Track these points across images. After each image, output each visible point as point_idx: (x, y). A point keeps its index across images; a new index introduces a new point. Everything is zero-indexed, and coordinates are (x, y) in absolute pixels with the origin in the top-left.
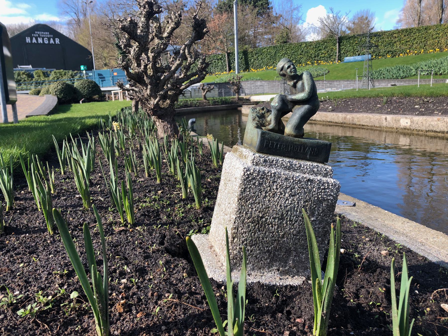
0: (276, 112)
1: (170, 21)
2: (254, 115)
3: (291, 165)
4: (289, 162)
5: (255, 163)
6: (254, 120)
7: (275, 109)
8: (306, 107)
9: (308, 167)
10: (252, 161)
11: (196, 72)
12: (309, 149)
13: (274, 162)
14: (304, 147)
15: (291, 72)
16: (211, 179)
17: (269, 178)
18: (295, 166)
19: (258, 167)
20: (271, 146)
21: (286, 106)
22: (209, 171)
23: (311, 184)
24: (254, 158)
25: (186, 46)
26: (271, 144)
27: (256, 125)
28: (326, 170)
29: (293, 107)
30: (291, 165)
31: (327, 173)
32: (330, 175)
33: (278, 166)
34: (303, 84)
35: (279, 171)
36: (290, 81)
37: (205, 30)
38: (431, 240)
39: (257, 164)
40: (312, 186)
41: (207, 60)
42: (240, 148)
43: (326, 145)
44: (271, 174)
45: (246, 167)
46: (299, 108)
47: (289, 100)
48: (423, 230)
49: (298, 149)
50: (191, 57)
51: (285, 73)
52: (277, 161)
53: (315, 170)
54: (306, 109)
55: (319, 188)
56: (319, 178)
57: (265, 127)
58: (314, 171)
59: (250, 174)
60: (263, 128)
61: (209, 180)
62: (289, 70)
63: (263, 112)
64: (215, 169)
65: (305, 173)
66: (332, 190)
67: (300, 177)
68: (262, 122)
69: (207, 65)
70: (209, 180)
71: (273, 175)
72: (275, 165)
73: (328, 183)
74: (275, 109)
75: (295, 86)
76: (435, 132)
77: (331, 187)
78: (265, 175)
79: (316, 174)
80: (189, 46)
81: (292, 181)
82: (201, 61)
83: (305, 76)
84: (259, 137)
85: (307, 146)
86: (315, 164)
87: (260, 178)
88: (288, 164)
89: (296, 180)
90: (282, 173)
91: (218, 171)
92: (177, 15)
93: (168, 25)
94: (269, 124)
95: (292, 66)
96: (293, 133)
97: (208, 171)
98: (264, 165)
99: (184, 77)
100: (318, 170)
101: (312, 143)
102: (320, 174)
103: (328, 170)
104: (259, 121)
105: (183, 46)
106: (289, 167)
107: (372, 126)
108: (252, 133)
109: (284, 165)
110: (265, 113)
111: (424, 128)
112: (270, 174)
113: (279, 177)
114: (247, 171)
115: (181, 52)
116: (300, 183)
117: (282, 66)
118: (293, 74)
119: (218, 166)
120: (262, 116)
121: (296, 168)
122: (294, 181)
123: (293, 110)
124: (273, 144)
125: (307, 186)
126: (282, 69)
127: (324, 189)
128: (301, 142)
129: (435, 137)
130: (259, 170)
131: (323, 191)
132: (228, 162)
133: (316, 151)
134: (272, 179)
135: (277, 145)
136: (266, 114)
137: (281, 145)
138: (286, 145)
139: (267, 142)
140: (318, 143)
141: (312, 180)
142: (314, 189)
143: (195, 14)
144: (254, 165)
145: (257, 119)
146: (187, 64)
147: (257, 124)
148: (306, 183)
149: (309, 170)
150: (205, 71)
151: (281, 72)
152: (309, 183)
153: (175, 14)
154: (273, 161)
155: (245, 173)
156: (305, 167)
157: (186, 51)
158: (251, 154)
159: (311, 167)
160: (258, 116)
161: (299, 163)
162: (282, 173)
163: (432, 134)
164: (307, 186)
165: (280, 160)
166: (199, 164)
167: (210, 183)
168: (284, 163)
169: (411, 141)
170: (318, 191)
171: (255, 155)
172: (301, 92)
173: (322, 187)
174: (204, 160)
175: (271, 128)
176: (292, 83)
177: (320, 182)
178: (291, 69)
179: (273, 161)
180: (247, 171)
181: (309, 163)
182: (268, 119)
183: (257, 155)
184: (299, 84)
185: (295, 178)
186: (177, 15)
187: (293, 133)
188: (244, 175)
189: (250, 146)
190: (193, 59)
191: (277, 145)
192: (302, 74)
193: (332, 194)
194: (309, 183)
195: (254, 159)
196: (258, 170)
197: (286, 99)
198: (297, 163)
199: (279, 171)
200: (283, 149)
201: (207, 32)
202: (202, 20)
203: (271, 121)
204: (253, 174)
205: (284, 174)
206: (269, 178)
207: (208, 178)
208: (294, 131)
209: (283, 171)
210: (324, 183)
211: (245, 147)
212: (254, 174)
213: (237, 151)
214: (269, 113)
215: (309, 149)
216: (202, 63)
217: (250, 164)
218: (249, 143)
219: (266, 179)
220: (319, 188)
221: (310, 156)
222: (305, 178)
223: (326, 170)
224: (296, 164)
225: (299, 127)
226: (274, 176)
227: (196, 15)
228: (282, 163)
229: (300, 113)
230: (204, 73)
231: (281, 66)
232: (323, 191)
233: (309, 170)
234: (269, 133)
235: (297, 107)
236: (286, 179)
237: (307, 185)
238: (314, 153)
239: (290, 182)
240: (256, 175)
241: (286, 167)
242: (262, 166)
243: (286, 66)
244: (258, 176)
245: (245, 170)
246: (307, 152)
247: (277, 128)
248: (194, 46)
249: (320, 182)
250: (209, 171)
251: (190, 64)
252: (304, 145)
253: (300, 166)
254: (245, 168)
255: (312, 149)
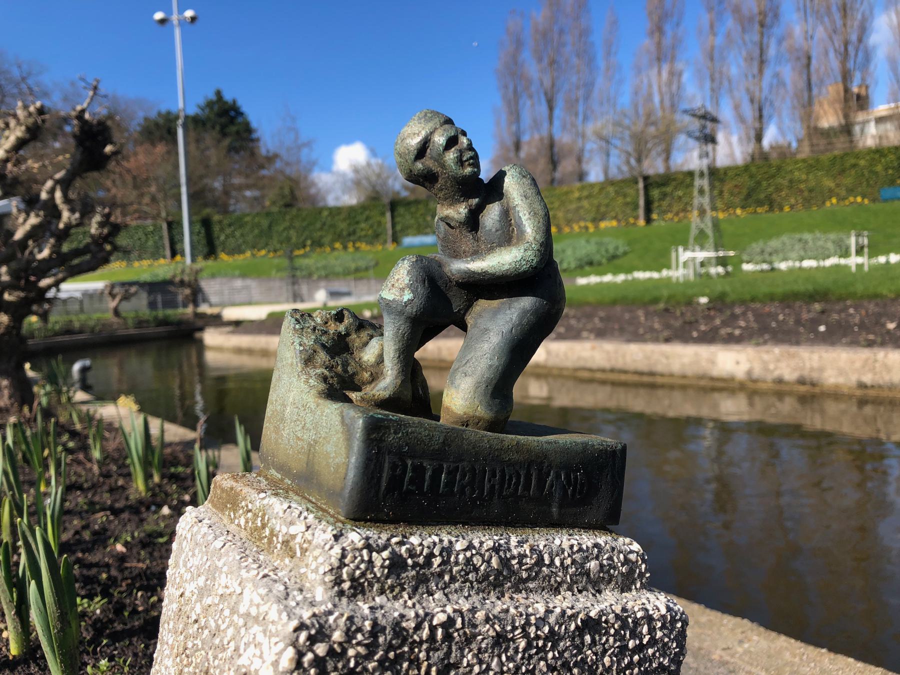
0: (404, 327)
1: (12, 122)
2: (309, 341)
3: (505, 562)
4: (496, 549)
5: (346, 586)
6: (308, 361)
7: (401, 313)
8: (526, 303)
9: (568, 561)
10: (329, 578)
11: (87, 246)
12: (558, 476)
13: (437, 561)
14: (540, 470)
15: (460, 162)
16: (126, 544)
17: (422, 655)
18: (520, 563)
19: (365, 608)
20: (412, 481)
21: (441, 306)
22: (122, 511)
23: (593, 640)
24: (343, 556)
25: (57, 182)
26: (409, 477)
27: (322, 386)
28: (627, 561)
29: (469, 306)
30: (505, 562)
31: (631, 571)
32: (641, 575)
33: (453, 579)
34: (507, 214)
35: (465, 606)
36: (453, 201)
37: (108, 149)
38: (740, 650)
39: (358, 589)
40: (599, 648)
41: (117, 218)
42: (253, 495)
43: (614, 452)
44: (433, 629)
45: (306, 614)
46: (496, 312)
47: (456, 277)
48: (703, 619)
49: (517, 484)
50: (72, 211)
51: (436, 168)
52: (447, 551)
53: (593, 565)
54: (524, 312)
55: (623, 649)
56: (609, 601)
57: (359, 389)
58: (587, 573)
59: (331, 652)
60: (353, 395)
61: (120, 548)
62: (451, 155)
63: (342, 328)
64: (141, 502)
65: (556, 591)
66: (665, 644)
67: (552, 619)
68: (346, 371)
69: (116, 229)
70: (120, 548)
71: (440, 632)
72: (441, 575)
73: (649, 619)
74: (401, 313)
75: (473, 222)
76: (591, 370)
77: (659, 634)
78: (404, 641)
79: (596, 584)
80: (65, 184)
81: (522, 644)
82: (97, 218)
83: (512, 185)
84: (357, 444)
85: (550, 466)
86: (587, 540)
87: (381, 662)
88: (494, 562)
89: (538, 637)
90: (480, 615)
91: (148, 508)
92: (32, 109)
93: (7, 133)
94: (375, 378)
95: (464, 141)
96: (482, 412)
97: (116, 512)
98: (392, 588)
99: (50, 255)
100: (602, 566)
101: (566, 451)
102: (609, 582)
103: (633, 557)
104: (330, 368)
105: (49, 184)
106: (499, 573)
107: (577, 370)
108: (308, 421)
109: (476, 570)
110: (348, 334)
111: (569, 364)
112: (425, 633)
113: (469, 640)
114: (313, 640)
115: (44, 196)
116: (553, 648)
117: (423, 134)
118: (468, 170)
119: (148, 489)
120: (339, 347)
121: (524, 575)
122: (529, 646)
123: (470, 320)
124: (419, 470)
125: (580, 652)
126: (422, 150)
127: (640, 648)
128: (529, 451)
129: (591, 381)
130: (375, 623)
131: (636, 658)
132: (195, 561)
133: (582, 485)
134: (436, 656)
135: (437, 473)
136: (354, 336)
137: (451, 473)
138: (473, 469)
139: (394, 467)
140: (585, 445)
141: (598, 622)
142: (607, 660)
143: (79, 108)
144: (341, 593)
145: (322, 356)
146: (61, 226)
147: (325, 379)
148: (578, 641)
149: (572, 570)
150: (111, 243)
151: (419, 165)
152: (588, 638)
153: (26, 107)
154: (431, 555)
155: (300, 654)
156: (557, 562)
157: (58, 195)
158: (324, 534)
159: (577, 557)
160: (323, 346)
161: (532, 549)
162: (480, 615)
163: (586, 375)
164: (580, 652)
165: (459, 546)
166: (89, 489)
167: (122, 558)
168: (477, 560)
169: (550, 391)
170: (619, 662)
171: (345, 542)
172: (500, 245)
173: (631, 644)
174: (107, 475)
175: (386, 394)
176: (459, 211)
177: (624, 626)
178: (461, 152)
179: (431, 555)
180: (313, 640)
181: (563, 540)
182: (369, 355)
183: (354, 537)
184: (492, 215)
185: (532, 630)
186: (32, 109)
187: (482, 412)
188: (299, 664)
189: (302, 482)
190: (77, 215)
191: (437, 473)
192: (500, 177)
193: (666, 662)
194: (588, 638)
195: (342, 565)
196: (367, 625)
197: (442, 275)
198: (526, 548)
199: (465, 606)
200: (462, 491)
201: (115, 153)
202: (101, 123)
203: (380, 360)
204: (344, 651)
205: (487, 620)
206: (422, 655)
207: (116, 540)
208: (489, 406)
209: (475, 599)
210: (636, 622)
211: (277, 489)
212: (351, 652)
213: (235, 507)
214: (364, 335)
215: (558, 476)
216: (101, 225)
217: (321, 594)
218: (297, 466)
219: (411, 662)
220: (623, 649)
221: (561, 507)
222: (570, 617)
223: (627, 561)
224: (522, 556)
225: (500, 387)
226: (448, 637)
227: (83, 111)
228: (468, 561)
229: (506, 329)
230: (108, 247)
231: (414, 142)
232: (636, 658)
233: (572, 570)
234: (400, 424)
235: (482, 305)
236: (501, 640)
237: (580, 649)
238: (573, 494)
239: (516, 651)
240: (361, 649)
241: (486, 577)
242: (382, 592)
243: (440, 139)
244: (369, 657)
245: (303, 636)
246: (551, 494)
247: (408, 394)
248: (78, 183)
249: (624, 626)
250: (122, 511)
251: (69, 227)
252: (538, 462)
253: (540, 562)
254: (298, 629)
255: (568, 477)
